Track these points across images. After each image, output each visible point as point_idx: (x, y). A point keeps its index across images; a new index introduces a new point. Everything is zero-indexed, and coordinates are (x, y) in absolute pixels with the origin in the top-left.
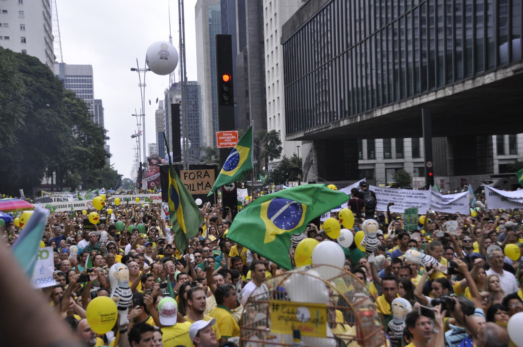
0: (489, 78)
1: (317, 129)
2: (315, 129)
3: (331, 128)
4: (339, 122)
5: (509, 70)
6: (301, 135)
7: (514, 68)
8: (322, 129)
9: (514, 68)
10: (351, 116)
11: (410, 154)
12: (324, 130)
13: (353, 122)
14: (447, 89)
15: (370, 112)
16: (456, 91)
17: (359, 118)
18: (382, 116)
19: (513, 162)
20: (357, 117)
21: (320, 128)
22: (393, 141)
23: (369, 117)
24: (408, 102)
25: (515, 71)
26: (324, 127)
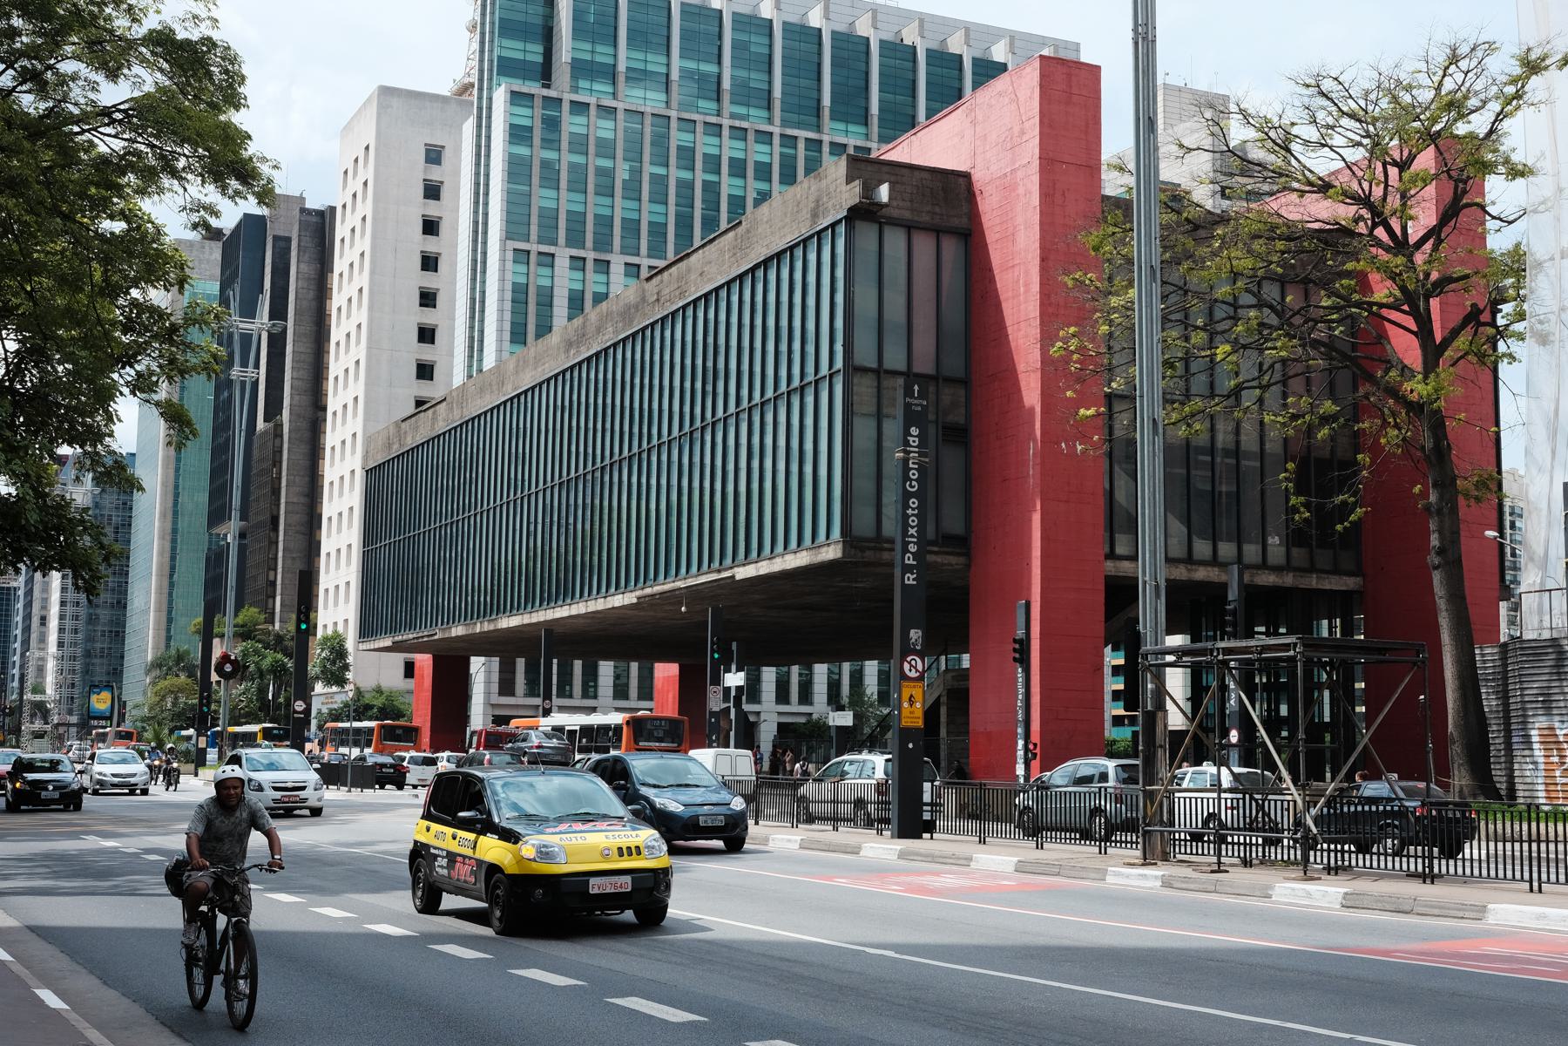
0: (618, 601)
1: (415, 635)
2: (411, 636)
3: (436, 637)
4: (450, 628)
5: (634, 594)
6: (388, 642)
7: (639, 593)
8: (422, 637)
9: (639, 593)
10: (468, 622)
11: (610, 692)
12: (425, 639)
13: (470, 632)
14: (580, 604)
15: (493, 620)
16: (589, 610)
17: (479, 625)
18: (509, 629)
19: (802, 720)
20: (475, 624)
21: (420, 634)
22: (578, 665)
23: (492, 627)
24: (540, 613)
25: (638, 598)
26: (426, 633)
